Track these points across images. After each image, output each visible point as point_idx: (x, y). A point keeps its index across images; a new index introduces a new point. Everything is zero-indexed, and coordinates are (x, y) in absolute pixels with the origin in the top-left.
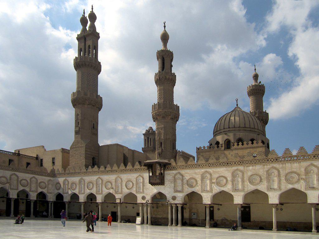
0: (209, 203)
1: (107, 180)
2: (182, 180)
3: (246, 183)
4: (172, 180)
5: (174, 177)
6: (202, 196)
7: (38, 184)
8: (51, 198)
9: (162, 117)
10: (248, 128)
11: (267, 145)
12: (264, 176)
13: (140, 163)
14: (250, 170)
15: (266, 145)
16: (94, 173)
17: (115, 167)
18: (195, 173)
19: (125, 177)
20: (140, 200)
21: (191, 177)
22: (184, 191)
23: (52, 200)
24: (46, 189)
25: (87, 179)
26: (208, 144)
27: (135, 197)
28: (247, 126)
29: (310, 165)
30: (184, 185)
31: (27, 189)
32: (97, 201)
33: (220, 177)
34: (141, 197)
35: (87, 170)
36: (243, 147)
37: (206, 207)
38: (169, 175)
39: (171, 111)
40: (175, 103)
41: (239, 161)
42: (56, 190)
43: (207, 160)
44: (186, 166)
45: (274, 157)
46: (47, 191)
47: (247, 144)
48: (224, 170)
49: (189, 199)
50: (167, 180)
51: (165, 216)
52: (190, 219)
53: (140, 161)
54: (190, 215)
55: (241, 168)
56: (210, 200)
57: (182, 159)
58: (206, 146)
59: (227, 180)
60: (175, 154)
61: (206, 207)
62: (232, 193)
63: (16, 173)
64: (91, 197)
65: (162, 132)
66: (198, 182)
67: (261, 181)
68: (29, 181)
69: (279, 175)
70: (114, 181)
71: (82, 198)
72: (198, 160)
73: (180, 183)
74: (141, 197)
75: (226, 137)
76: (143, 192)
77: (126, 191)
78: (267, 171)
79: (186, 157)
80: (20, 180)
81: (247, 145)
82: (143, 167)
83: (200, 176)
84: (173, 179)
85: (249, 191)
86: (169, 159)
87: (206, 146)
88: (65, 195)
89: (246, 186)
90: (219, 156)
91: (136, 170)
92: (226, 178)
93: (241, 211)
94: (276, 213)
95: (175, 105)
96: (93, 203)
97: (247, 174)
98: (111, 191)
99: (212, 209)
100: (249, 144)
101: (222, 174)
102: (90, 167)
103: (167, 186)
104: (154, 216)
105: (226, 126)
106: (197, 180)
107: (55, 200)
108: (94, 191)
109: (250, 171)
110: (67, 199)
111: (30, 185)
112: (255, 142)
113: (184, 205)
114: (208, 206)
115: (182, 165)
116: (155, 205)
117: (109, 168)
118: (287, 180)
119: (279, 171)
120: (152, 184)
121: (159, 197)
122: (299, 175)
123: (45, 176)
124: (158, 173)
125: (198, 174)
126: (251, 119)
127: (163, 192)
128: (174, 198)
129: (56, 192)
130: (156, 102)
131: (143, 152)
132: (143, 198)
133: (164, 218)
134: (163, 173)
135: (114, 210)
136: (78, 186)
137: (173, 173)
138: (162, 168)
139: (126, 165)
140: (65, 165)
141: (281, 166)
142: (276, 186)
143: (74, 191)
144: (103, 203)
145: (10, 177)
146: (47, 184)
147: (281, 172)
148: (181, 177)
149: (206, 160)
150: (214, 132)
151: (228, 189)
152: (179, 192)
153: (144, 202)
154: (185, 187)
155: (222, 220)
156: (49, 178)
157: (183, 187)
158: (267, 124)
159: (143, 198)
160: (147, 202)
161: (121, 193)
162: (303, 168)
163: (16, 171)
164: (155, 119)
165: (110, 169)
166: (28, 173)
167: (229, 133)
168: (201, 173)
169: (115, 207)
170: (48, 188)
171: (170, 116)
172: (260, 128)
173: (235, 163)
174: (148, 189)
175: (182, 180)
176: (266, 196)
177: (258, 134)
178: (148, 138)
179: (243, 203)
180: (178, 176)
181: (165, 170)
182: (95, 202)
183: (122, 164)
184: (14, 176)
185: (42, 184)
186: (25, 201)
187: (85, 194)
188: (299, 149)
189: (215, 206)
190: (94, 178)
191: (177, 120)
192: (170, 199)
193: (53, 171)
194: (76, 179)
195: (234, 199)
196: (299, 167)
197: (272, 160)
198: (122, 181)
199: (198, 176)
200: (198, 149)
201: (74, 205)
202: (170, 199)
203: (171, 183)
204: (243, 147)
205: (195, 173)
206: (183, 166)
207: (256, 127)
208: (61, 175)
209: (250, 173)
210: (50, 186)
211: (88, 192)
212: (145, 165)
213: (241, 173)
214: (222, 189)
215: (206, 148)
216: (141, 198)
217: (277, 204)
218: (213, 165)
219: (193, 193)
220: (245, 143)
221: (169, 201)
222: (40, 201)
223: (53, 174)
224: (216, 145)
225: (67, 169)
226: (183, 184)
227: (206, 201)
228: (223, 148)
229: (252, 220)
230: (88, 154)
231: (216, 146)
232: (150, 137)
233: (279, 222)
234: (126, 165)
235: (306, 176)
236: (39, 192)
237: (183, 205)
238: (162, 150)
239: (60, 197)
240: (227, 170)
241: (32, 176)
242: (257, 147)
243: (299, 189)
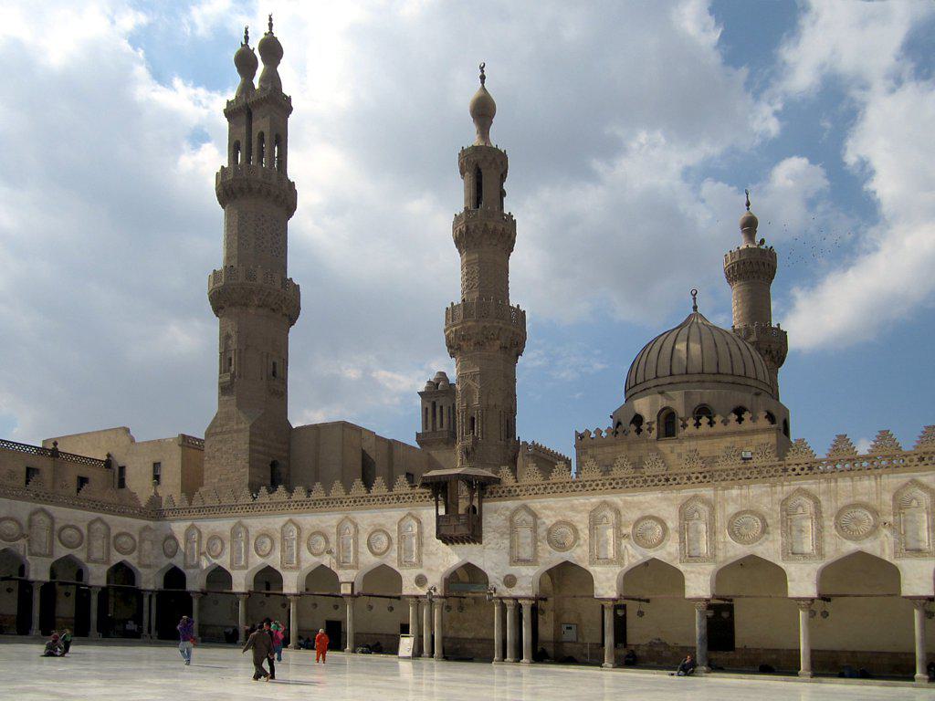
0: (614, 595)
1: (313, 527)
2: (535, 529)
3: (720, 538)
4: (505, 527)
5: (511, 520)
6: (592, 573)
7: (112, 539)
8: (150, 580)
9: (475, 344)
10: (727, 374)
11: (782, 426)
12: (774, 517)
13: (410, 477)
14: (734, 498)
15: (779, 424)
16: (276, 508)
17: (337, 491)
18: (573, 508)
19: (367, 518)
20: (409, 588)
21: (560, 518)
22: (539, 560)
23: (151, 587)
24: (135, 554)
25: (256, 524)
26: (610, 423)
27: (396, 578)
28: (725, 368)
29: (907, 484)
30: (539, 543)
31: (80, 555)
32: (285, 591)
33: (644, 518)
34: (412, 579)
35: (254, 498)
36: (712, 430)
37: (603, 606)
38: (495, 513)
39: (501, 325)
40: (513, 302)
41: (701, 473)
42: (165, 558)
43: (607, 470)
44: (545, 488)
45: (802, 461)
46: (136, 561)
47: (725, 422)
48: (658, 498)
49: (553, 584)
50: (489, 529)
51: (483, 633)
52: (558, 643)
53: (411, 472)
54: (557, 630)
55: (707, 492)
56: (615, 586)
57: (532, 467)
58: (604, 429)
59: (665, 529)
60: (512, 452)
61: (603, 606)
62: (681, 567)
63: (46, 507)
64: (268, 579)
65: (476, 386)
66: (581, 534)
67: (765, 530)
68: (85, 532)
69: (818, 514)
70: (335, 530)
71: (241, 582)
72: (582, 469)
73: (526, 537)
74: (414, 577)
75: (662, 402)
76: (420, 563)
77: (369, 560)
78: (784, 503)
79: (546, 460)
80: (57, 527)
81: (725, 425)
82: (418, 490)
83: (588, 515)
84: (508, 524)
85: (731, 561)
86: (495, 465)
87: (604, 429)
88: (192, 571)
89: (721, 546)
90: (640, 457)
91: (398, 499)
92: (662, 522)
93: (708, 618)
94: (810, 625)
95: (513, 307)
96: (272, 596)
97: (724, 511)
98: (327, 560)
99: (620, 613)
100: (729, 421)
101: (652, 512)
102: (263, 489)
103: (490, 546)
104: (451, 634)
105: (664, 370)
106: (579, 528)
107: (162, 587)
108: (275, 561)
109: (733, 501)
110: (195, 583)
111: (89, 544)
112: (746, 416)
113: (540, 602)
114: (611, 603)
115: (533, 483)
116: (453, 602)
117: (318, 493)
118: (841, 528)
119: (817, 503)
120: (446, 539)
121: (467, 579)
122: (875, 512)
123: (133, 516)
124: (463, 506)
125: (582, 511)
126: (734, 349)
127: (478, 563)
128: (510, 581)
129: (165, 562)
130: (458, 300)
131: (418, 447)
132: (421, 581)
133: (482, 640)
134: (477, 508)
135: (334, 616)
136: (228, 546)
137: (508, 509)
138: (476, 494)
139: (368, 484)
140: (191, 484)
141: (823, 486)
142: (808, 546)
143: (217, 561)
144: (300, 595)
145: (30, 520)
146: (137, 540)
147: (824, 503)
148: (530, 519)
149: (604, 469)
150: (628, 388)
151: (669, 554)
152: (526, 562)
153: (423, 592)
154: (542, 550)
155: (651, 645)
156: (144, 523)
157: (535, 549)
158: (782, 362)
159: (421, 581)
160: (432, 591)
161: (355, 567)
162: (888, 492)
163: (46, 502)
164: (454, 348)
165: (322, 496)
166: (83, 508)
167: (673, 390)
168: (590, 509)
169: (336, 607)
170: (140, 552)
171: (498, 339)
172: (761, 377)
173: (689, 478)
174: (433, 554)
175: (535, 529)
176: (779, 576)
177: (757, 394)
178: (434, 404)
179: (714, 595)
180: (523, 515)
181: (483, 497)
182: (280, 592)
183: (358, 482)
184: (41, 518)
185: (124, 539)
186: (72, 590)
187: (250, 569)
188: (877, 437)
189: (629, 604)
190: (275, 522)
191: (519, 353)
192: (499, 582)
193: (155, 501)
194: (223, 525)
195: (687, 583)
196: (875, 489)
197: (798, 469)
198: (357, 531)
199: (580, 515)
200: (580, 437)
201: (216, 603)
202: (499, 582)
203: (502, 536)
204: (712, 430)
205: (573, 508)
206: (536, 486)
207: (751, 373)
208: (178, 513)
209: (732, 509)
210: (147, 545)
211: (257, 562)
212: (424, 485)
213: (706, 508)
214: (652, 554)
215: (604, 434)
216: (413, 581)
217: (812, 600)
218: (624, 483)
219: (566, 567)
220: (718, 419)
221: (495, 590)
222: (116, 589)
223: (155, 511)
224: (632, 425)
225: (197, 494)
226: (535, 540)
227: (603, 589)
228: (654, 434)
229: (737, 645)
230: (259, 452)
231: (634, 427)
232: (441, 401)
233: (819, 651)
234: (368, 484)
235: (897, 518)
236: (114, 563)
237: (537, 603)
238: (475, 439)
239: (175, 577)
240: (666, 499)
241: (93, 515)
242: (754, 432)
243: (877, 553)
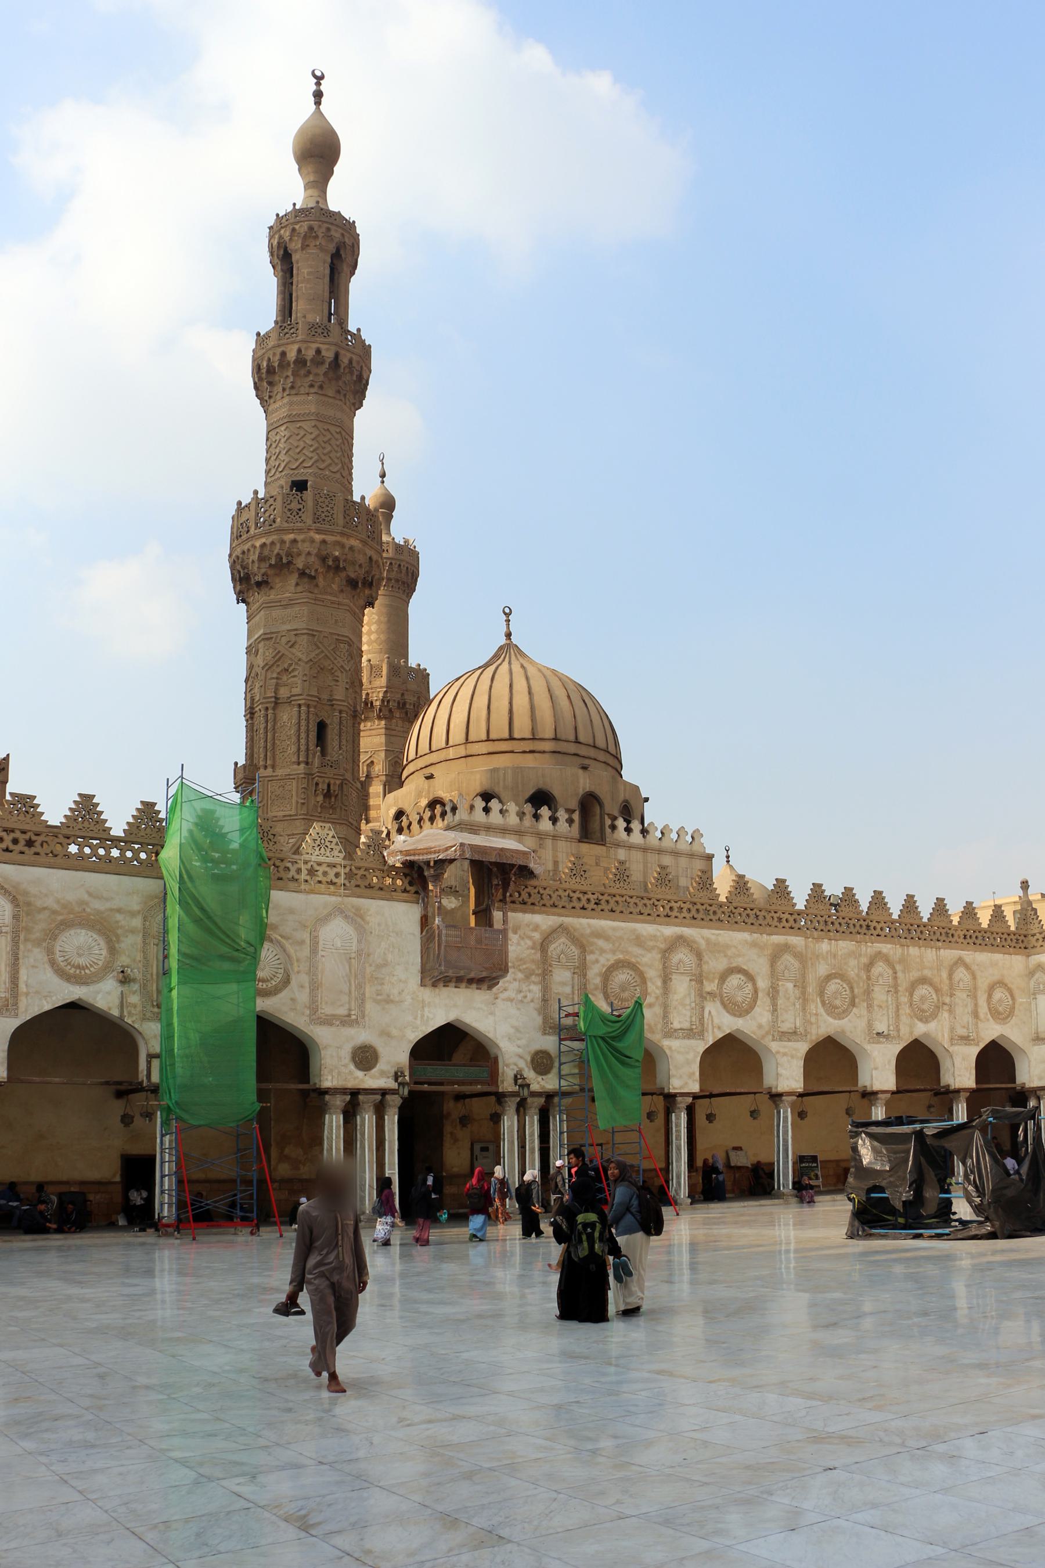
2: (581, 970)
21: (621, 956)
84: (538, 956)
103: (505, 995)
125: (653, 948)
137: (536, 928)
168: (663, 946)
199: (649, 955)
203: (527, 977)
205: (639, 941)
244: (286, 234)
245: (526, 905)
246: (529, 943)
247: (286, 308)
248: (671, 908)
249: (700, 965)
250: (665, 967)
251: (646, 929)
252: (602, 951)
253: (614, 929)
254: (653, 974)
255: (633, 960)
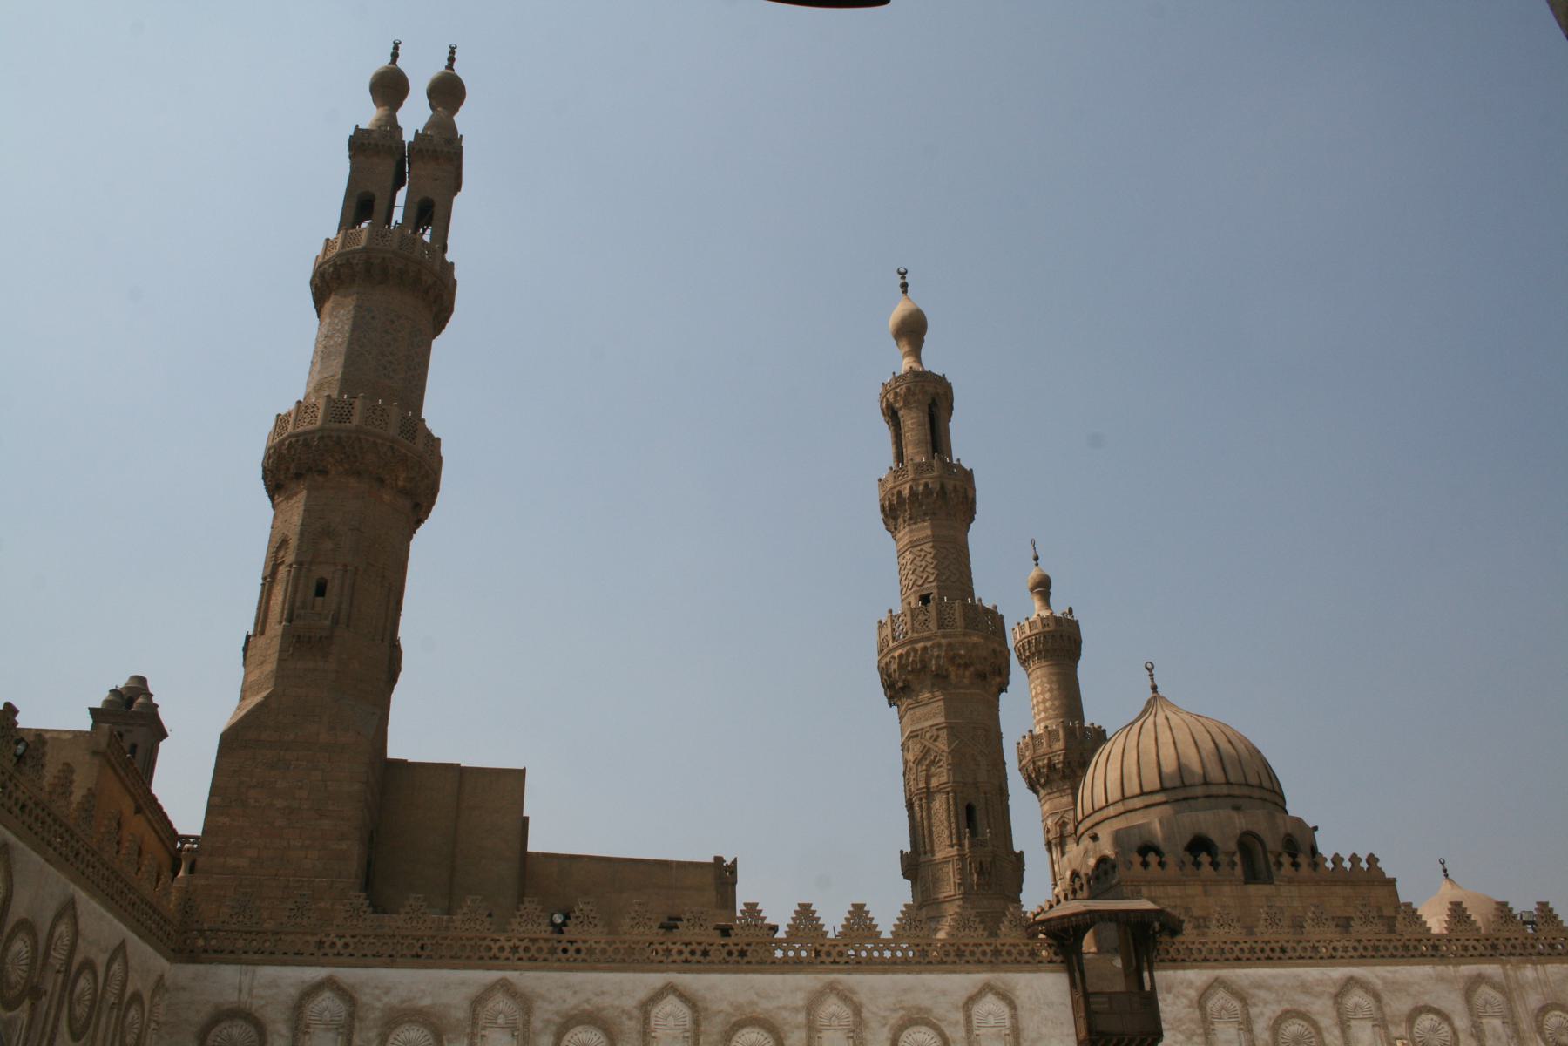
2: (1247, 1025)
4: (1192, 1020)
21: (1288, 1006)
83: (1330, 1003)
137: (1190, 984)
148: (1235, 1005)
168: (1334, 990)
175: (1247, 1025)
205: (1305, 988)
244: (891, 397)
245: (1176, 962)
246: (1185, 1001)
247: (899, 456)
248: (1334, 949)
249: (1380, 1008)
250: (1339, 1014)
251: (1311, 973)
252: (1266, 1003)
253: (1274, 977)
254: (1327, 1021)
255: (1302, 1009)
